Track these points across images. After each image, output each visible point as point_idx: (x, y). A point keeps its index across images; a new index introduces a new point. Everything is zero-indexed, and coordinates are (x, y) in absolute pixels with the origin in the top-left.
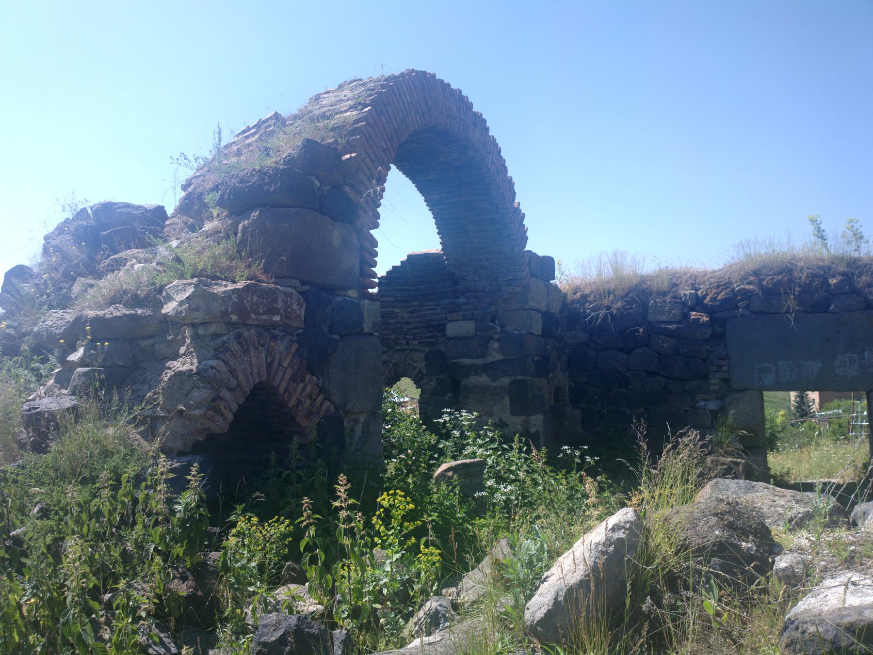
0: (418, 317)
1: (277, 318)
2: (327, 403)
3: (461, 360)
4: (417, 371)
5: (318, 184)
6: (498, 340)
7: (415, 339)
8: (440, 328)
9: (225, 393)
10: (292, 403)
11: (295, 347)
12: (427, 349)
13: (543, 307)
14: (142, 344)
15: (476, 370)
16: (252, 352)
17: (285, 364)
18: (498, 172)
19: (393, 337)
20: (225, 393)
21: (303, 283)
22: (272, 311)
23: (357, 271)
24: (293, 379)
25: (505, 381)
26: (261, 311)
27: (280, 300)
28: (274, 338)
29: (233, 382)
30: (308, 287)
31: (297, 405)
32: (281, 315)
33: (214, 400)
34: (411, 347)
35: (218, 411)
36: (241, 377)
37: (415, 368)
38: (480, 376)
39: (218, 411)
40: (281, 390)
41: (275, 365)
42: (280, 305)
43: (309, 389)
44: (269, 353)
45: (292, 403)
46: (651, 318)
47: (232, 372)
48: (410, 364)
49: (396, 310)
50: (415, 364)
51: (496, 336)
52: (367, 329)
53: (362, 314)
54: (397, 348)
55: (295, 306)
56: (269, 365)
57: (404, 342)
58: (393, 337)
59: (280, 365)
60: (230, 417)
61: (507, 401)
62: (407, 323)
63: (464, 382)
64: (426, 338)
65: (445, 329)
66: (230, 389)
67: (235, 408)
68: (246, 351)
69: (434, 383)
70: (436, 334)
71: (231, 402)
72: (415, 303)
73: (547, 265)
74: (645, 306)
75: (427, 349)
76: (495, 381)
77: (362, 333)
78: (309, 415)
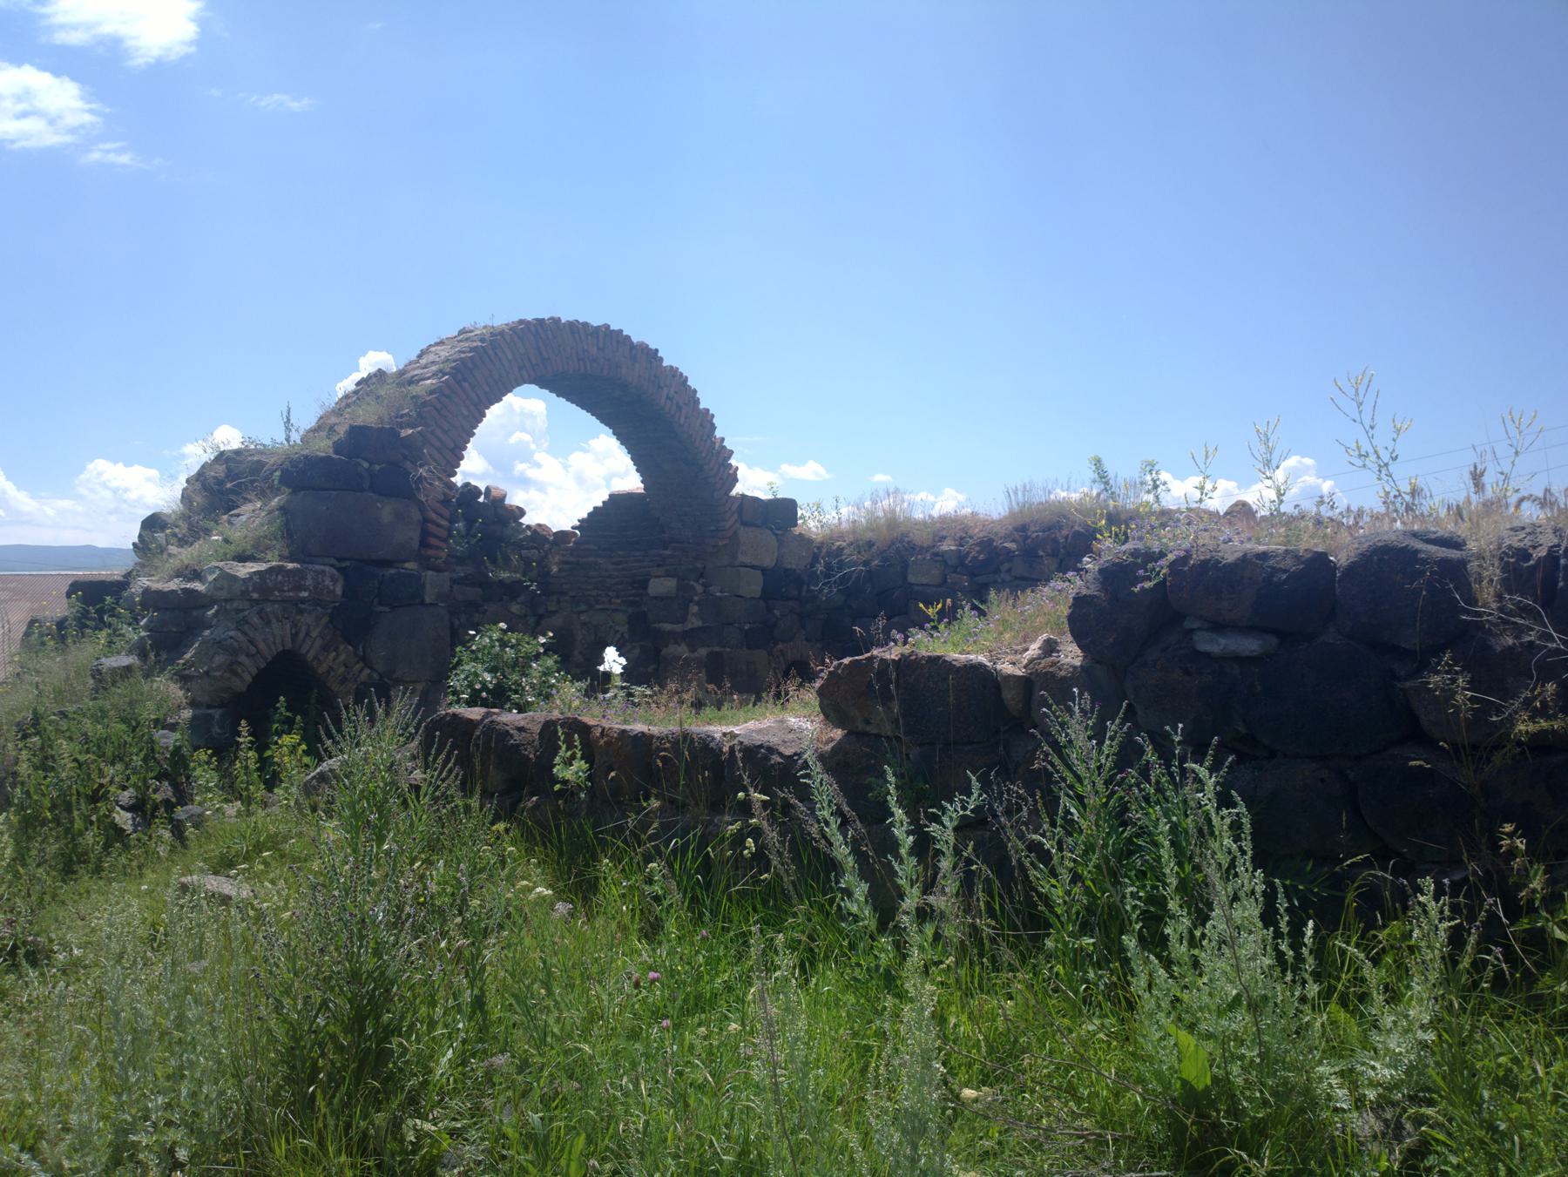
1: (305, 594)
2: (367, 671)
5: (366, 465)
6: (698, 603)
8: (644, 584)
9: (243, 658)
10: (322, 669)
11: (325, 620)
12: (630, 610)
13: (768, 561)
14: (195, 613)
15: (677, 638)
16: (275, 625)
17: (314, 634)
18: (679, 408)
19: (594, 593)
20: (243, 658)
21: (339, 560)
22: (300, 588)
23: (415, 544)
24: (325, 648)
25: (703, 652)
28: (301, 612)
29: (253, 650)
33: (231, 664)
35: (235, 674)
36: (262, 646)
39: (235, 674)
40: (310, 657)
41: (302, 635)
42: (309, 582)
43: (342, 657)
45: (320, 671)
46: (911, 579)
47: (252, 641)
49: (600, 561)
52: (428, 600)
53: (423, 586)
56: (295, 636)
59: (307, 634)
60: (249, 679)
62: (610, 577)
63: (664, 651)
65: (645, 588)
66: (248, 655)
67: (254, 671)
68: (268, 623)
71: (249, 669)
73: (783, 511)
74: (905, 565)
75: (630, 610)
77: (422, 603)
78: (344, 680)
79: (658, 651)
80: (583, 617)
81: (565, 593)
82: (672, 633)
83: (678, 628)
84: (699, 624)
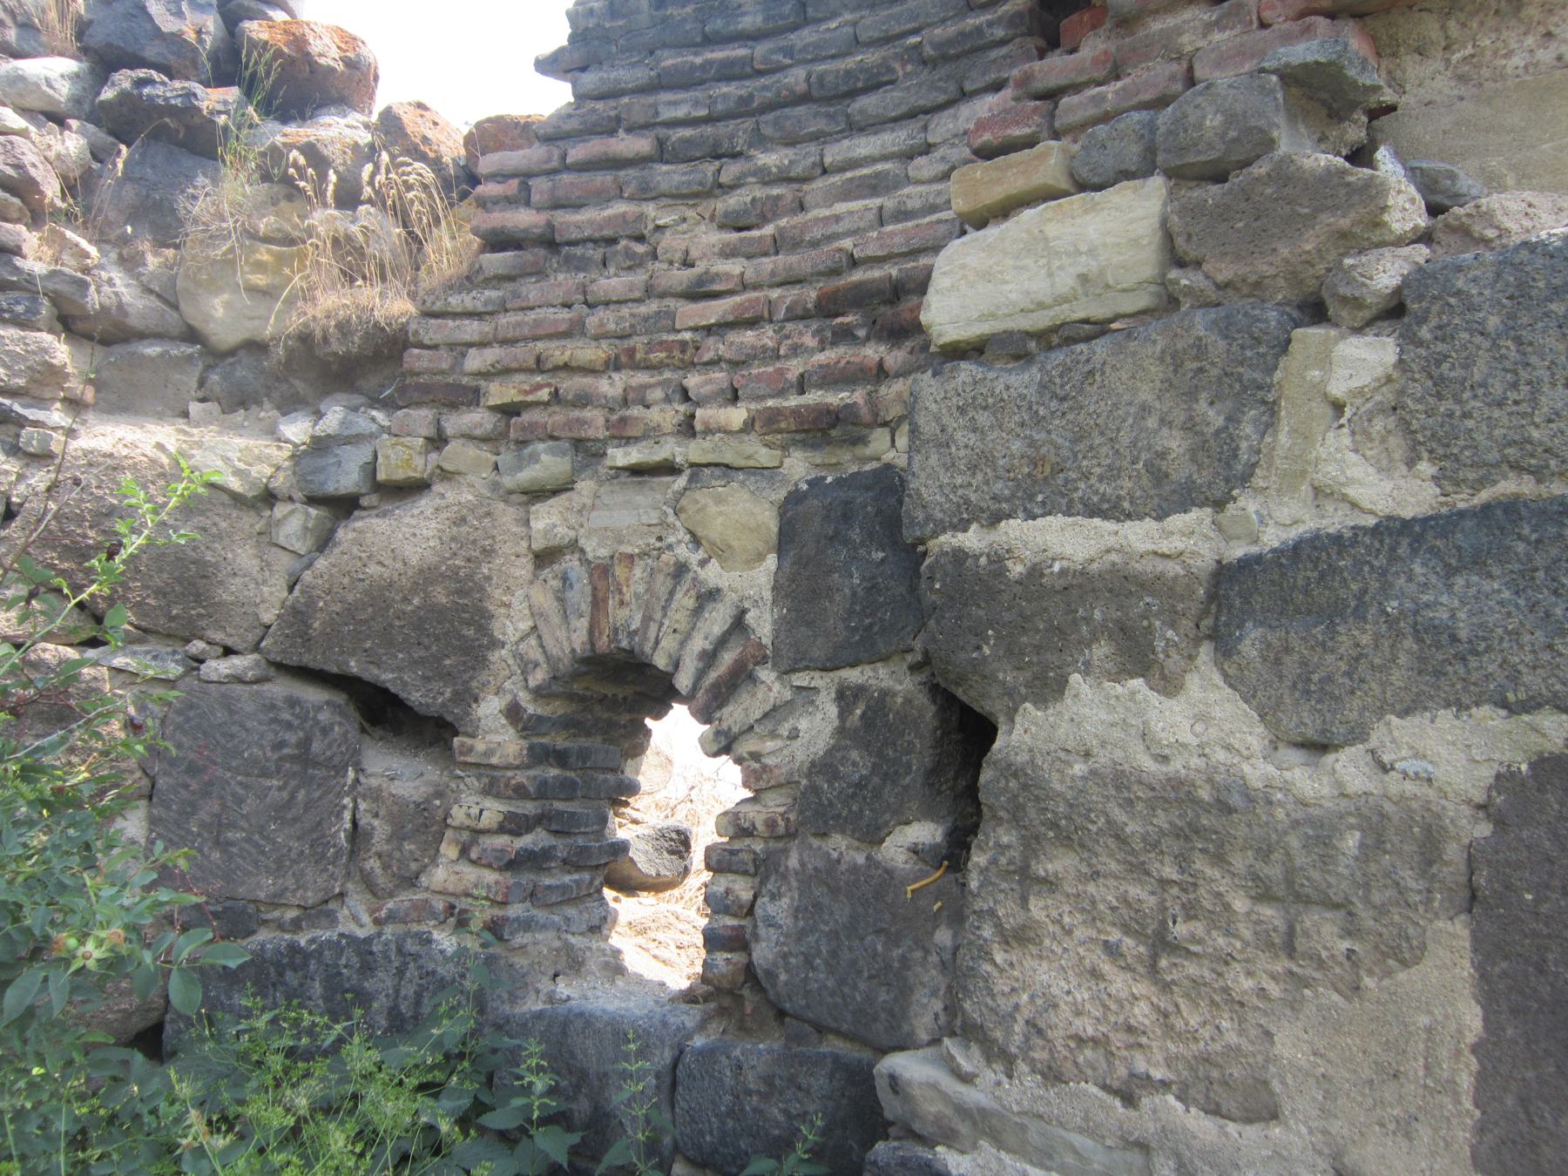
0: (777, 245)
3: (1014, 530)
4: (717, 620)
7: (734, 397)
12: (798, 467)
15: (1130, 624)
34: (696, 451)
37: (710, 596)
38: (1169, 686)
48: (681, 569)
50: (713, 574)
51: (1385, 273)
54: (621, 456)
57: (666, 416)
58: (610, 386)
61: (1445, 987)
63: (1023, 735)
64: (801, 386)
69: (817, 727)
70: (872, 352)
72: (770, 159)
75: (798, 467)
76: (1318, 747)
79: (969, 733)
80: (548, 520)
81: (473, 397)
82: (1119, 581)
83: (1184, 541)
84: (1383, 486)
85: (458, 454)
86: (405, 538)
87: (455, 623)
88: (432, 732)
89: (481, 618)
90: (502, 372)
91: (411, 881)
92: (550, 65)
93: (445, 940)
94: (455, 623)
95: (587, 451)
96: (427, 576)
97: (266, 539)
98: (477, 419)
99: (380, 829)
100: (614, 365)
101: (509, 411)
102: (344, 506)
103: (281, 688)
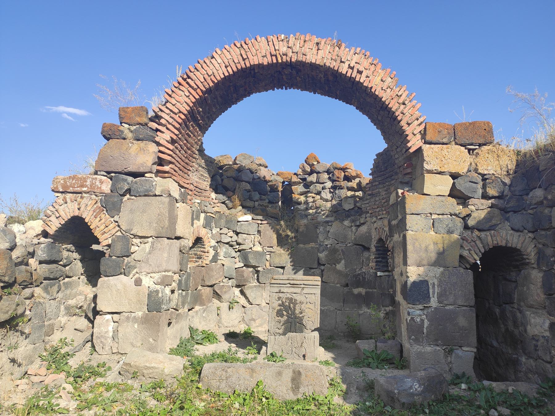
1: (85, 189)
26: (76, 186)
27: (88, 181)
30: (113, 174)
31: (96, 228)
32: (88, 188)
36: (62, 213)
40: (86, 221)
42: (88, 183)
44: (79, 204)
54: (379, 217)
55: (98, 183)
58: (377, 210)
77: (156, 195)
85: (368, 219)
86: (364, 229)
87: (369, 237)
88: (368, 249)
89: (371, 236)
90: (370, 210)
91: (368, 265)
92: (370, 175)
93: (371, 271)
94: (369, 237)
95: (376, 217)
96: (366, 233)
97: (352, 231)
98: (369, 215)
99: (365, 260)
100: (378, 208)
101: (371, 213)
102: (359, 226)
103: (355, 246)
